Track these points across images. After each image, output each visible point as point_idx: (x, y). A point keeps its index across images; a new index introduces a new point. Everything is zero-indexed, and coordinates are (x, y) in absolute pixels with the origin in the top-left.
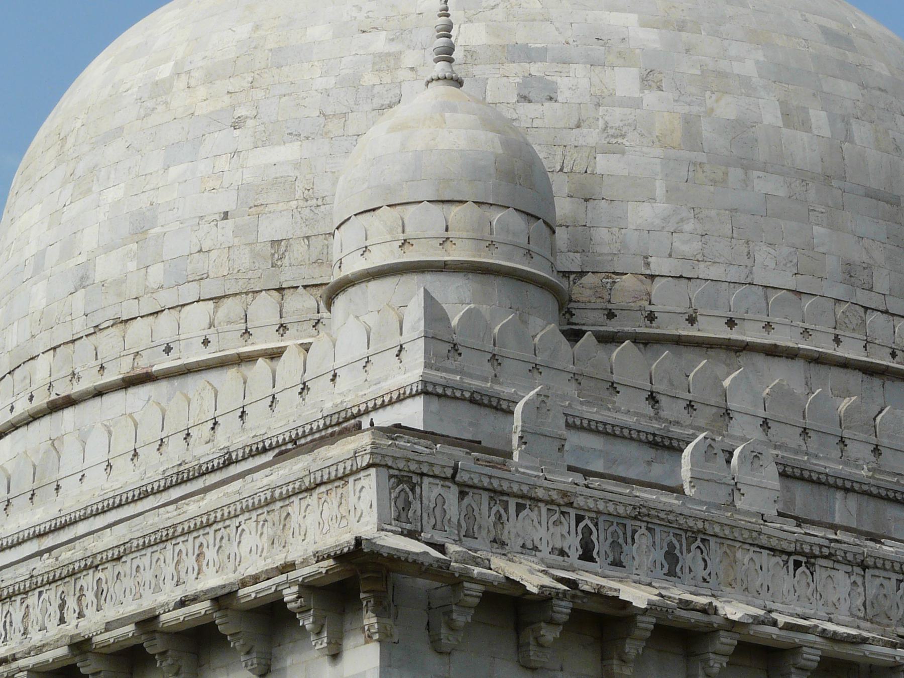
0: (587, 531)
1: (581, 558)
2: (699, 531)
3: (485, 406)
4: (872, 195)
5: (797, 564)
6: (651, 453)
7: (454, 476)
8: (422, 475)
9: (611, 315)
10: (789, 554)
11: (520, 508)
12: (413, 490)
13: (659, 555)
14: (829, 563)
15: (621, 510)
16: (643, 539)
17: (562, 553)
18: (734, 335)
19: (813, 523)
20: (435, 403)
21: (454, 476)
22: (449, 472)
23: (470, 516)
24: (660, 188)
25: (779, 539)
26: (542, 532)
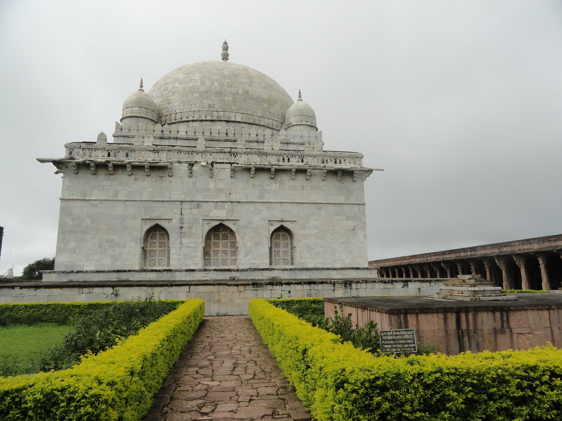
0: (109, 153)
4: (216, 93)
13: (125, 154)
16: (121, 152)
18: (188, 119)
20: (116, 138)
23: (85, 153)
24: (178, 100)
26: (100, 154)
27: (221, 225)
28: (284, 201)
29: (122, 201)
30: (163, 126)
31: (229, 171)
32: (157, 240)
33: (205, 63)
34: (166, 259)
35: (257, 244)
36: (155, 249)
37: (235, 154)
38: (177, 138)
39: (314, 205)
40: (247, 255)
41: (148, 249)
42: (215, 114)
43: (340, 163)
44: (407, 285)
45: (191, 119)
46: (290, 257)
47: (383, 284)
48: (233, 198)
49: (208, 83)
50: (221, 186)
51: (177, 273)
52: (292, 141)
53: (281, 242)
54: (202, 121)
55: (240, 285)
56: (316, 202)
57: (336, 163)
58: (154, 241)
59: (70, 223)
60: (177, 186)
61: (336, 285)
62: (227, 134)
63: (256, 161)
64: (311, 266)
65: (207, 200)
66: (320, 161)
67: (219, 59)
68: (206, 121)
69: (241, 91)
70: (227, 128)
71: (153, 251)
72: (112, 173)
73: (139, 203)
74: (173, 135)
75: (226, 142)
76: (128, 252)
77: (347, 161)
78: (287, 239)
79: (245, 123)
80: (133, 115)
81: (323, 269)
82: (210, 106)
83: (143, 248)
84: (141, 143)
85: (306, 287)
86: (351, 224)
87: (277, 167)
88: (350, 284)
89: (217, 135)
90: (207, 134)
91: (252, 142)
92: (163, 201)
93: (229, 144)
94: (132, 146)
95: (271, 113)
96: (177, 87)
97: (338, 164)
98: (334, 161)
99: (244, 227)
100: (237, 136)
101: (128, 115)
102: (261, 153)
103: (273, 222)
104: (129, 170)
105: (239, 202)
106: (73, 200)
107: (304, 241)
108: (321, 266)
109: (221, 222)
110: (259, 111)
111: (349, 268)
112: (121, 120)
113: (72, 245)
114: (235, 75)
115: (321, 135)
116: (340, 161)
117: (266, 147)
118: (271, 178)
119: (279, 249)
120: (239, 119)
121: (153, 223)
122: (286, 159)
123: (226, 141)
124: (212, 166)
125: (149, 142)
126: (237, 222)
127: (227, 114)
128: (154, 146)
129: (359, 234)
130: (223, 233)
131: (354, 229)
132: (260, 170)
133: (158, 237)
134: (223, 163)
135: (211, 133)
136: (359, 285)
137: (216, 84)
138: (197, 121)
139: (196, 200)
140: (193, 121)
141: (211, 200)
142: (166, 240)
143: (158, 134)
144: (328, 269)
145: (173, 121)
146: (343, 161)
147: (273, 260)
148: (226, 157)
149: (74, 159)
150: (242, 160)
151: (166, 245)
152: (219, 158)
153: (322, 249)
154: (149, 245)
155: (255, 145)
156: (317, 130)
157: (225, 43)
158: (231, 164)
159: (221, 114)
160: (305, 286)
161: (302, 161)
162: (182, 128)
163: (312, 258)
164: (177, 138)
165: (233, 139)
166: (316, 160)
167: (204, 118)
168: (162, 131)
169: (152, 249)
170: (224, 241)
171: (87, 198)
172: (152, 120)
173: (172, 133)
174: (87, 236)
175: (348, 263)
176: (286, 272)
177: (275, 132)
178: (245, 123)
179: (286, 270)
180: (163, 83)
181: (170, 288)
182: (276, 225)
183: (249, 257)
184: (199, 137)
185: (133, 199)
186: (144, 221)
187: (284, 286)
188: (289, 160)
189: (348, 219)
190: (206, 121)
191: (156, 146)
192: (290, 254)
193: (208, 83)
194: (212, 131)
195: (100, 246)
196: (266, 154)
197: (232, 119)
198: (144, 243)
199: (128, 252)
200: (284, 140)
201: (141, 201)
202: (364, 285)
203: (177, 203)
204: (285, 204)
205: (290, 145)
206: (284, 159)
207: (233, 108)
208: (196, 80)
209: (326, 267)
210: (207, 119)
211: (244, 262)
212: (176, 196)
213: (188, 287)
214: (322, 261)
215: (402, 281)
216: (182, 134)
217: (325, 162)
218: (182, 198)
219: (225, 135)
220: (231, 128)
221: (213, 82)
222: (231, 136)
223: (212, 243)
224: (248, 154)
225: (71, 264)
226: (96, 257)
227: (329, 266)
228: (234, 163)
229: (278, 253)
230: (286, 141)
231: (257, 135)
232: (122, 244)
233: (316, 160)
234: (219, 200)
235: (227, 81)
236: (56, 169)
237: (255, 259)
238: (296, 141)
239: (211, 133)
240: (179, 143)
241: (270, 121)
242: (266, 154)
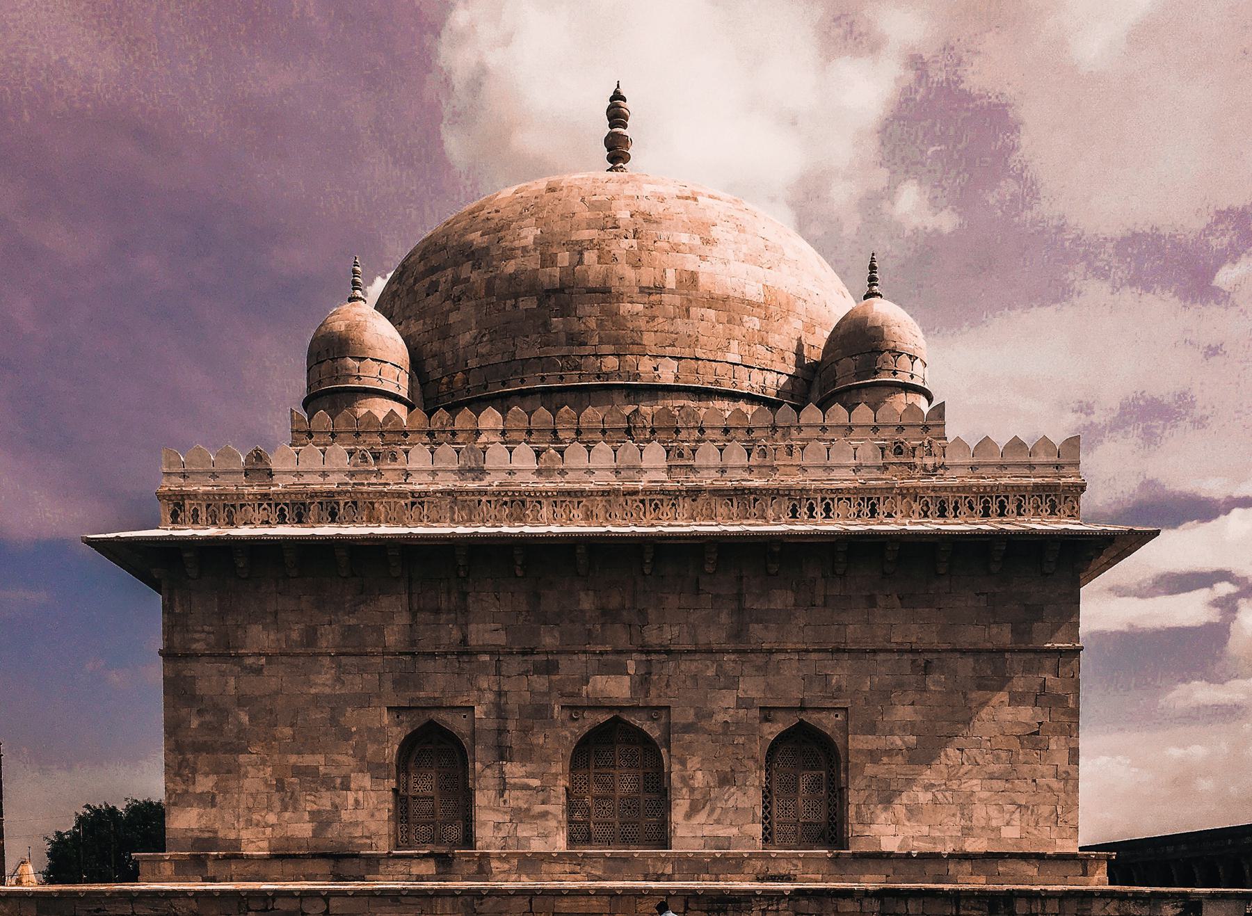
27: (616, 720)
35: (725, 780)
40: (693, 810)
59: (195, 723)
83: (395, 791)
96: (467, 280)
98: (979, 508)
99: (688, 728)
107: (870, 769)
110: (734, 344)
113: (205, 784)
114: (648, 218)
115: (942, 416)
116: (1002, 506)
121: (422, 719)
126: (664, 713)
129: (1053, 746)
153: (929, 796)
161: (873, 512)
163: (897, 823)
174: (243, 758)
175: (1011, 834)
180: (421, 267)
183: (701, 817)
193: (564, 258)
195: (280, 786)
198: (398, 781)
199: (357, 801)
203: (486, 658)
208: (524, 249)
214: (925, 830)
218: (501, 639)
221: (581, 253)
225: (206, 835)
226: (272, 818)
232: (339, 781)
237: (718, 822)
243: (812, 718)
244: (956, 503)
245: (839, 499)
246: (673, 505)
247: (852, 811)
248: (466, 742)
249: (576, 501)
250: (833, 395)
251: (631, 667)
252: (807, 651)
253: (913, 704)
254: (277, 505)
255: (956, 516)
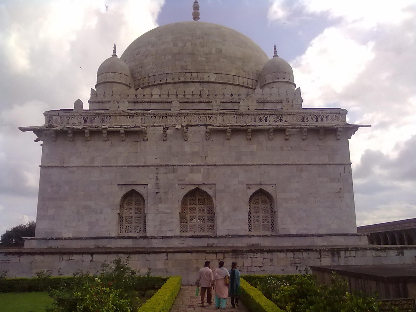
1: (84, 123)
2: (108, 115)
3: (140, 103)
5: (130, 117)
6: (134, 104)
7: (58, 115)
8: (53, 116)
9: (144, 84)
10: (128, 116)
11: (72, 118)
12: (51, 119)
13: (100, 120)
14: (137, 116)
15: (92, 115)
17: (80, 123)
18: (161, 82)
19: (133, 110)
21: (58, 115)
22: (57, 115)
25: (125, 114)
26: (77, 121)
27: (197, 189)
28: (262, 163)
29: (98, 167)
30: (136, 90)
31: (203, 133)
32: (133, 206)
33: (177, 25)
34: (142, 225)
35: (235, 209)
36: (130, 215)
37: (210, 116)
38: (150, 102)
39: (294, 167)
41: (125, 215)
42: (188, 75)
43: (322, 121)
44: (402, 254)
45: (164, 81)
46: (270, 223)
47: (374, 252)
48: (210, 160)
49: (180, 44)
50: (196, 149)
51: (154, 240)
52: (268, 99)
53: (261, 206)
54: (175, 83)
55: (219, 252)
56: (297, 163)
57: (317, 121)
58: (131, 207)
60: (152, 151)
61: (322, 253)
62: (200, 95)
63: (232, 121)
64: (293, 232)
65: (182, 164)
66: (300, 119)
67: (190, 19)
68: (179, 83)
69: (213, 51)
70: (201, 89)
71: (129, 217)
72: (88, 139)
73: (115, 168)
74: (147, 99)
75: (200, 104)
76: (105, 218)
77: (329, 118)
78: (266, 203)
79: (219, 83)
80: (108, 80)
81: (307, 235)
82: (182, 67)
83: (119, 214)
84: (116, 109)
85: (290, 255)
86: (336, 186)
87: (253, 127)
88: (338, 253)
89: (190, 97)
90: (181, 96)
91: (226, 102)
92: (138, 166)
93: (203, 106)
94: (107, 112)
95: (245, 71)
97: (319, 122)
98: (314, 119)
100: (211, 97)
101: (102, 81)
102: (237, 114)
103: (251, 186)
104: (105, 135)
105: (215, 165)
106: (52, 167)
108: (305, 232)
109: (197, 186)
111: (336, 235)
112: (96, 87)
116: (322, 118)
117: (242, 107)
118: (247, 139)
119: (258, 214)
120: (213, 80)
122: (263, 119)
123: (200, 102)
124: (187, 129)
125: (124, 106)
127: (200, 75)
128: (129, 111)
130: (200, 198)
131: (340, 192)
132: (236, 131)
133: (133, 203)
134: (198, 125)
135: (184, 95)
136: (348, 254)
137: (188, 44)
138: (170, 83)
139: (172, 164)
140: (166, 83)
141: (186, 164)
142: (142, 207)
143: (132, 98)
144: (313, 235)
145: (147, 85)
146: (324, 118)
147: (252, 226)
148: (201, 119)
149: (53, 127)
150: (218, 122)
151: (142, 211)
152: (194, 120)
154: (125, 212)
155: (230, 106)
156: (295, 86)
157: (196, 2)
158: (206, 126)
159: (195, 75)
160: (288, 253)
161: (281, 120)
162: (156, 92)
164: (150, 102)
165: (207, 100)
166: (295, 118)
167: (177, 80)
168: (136, 96)
169: (128, 215)
170: (200, 206)
171: (65, 165)
172: (126, 85)
173: (146, 97)
175: (334, 228)
176: (266, 239)
177: (250, 91)
178: (219, 83)
179: (267, 236)
181: (147, 256)
182: (254, 189)
184: (172, 100)
185: (109, 165)
186: (120, 187)
187: (266, 254)
188: (266, 119)
189: (332, 180)
190: (179, 83)
191: (131, 110)
192: (270, 220)
193: (180, 44)
194: (186, 93)
196: (242, 115)
197: (206, 80)
199: (105, 218)
200: (260, 98)
201: (117, 166)
202: (353, 253)
204: (263, 166)
205: (266, 104)
206: (261, 119)
207: (207, 68)
209: (310, 233)
210: (181, 80)
211: (222, 228)
212: (151, 160)
213: (165, 254)
215: (397, 248)
216: (156, 97)
217: (305, 120)
218: (158, 162)
219: (199, 97)
220: (205, 89)
221: (185, 43)
222: (205, 98)
223: (189, 209)
224: (222, 115)
227: (313, 232)
228: (209, 125)
229: (257, 218)
230: (262, 100)
231: (232, 95)
232: (99, 211)
233: (295, 118)
234: (195, 164)
235: (199, 41)
236: (36, 137)
238: (273, 99)
239: (184, 95)
240: (153, 106)
241: (245, 80)
242: (242, 115)
243: (265, 188)
244: (307, 117)
245: (270, 116)
246: (216, 118)
247: (279, 220)
248: (145, 196)
249: (184, 116)
250: (265, 85)
251: (202, 170)
252: (261, 165)
253: (298, 182)
254: (84, 117)
255: (307, 121)
